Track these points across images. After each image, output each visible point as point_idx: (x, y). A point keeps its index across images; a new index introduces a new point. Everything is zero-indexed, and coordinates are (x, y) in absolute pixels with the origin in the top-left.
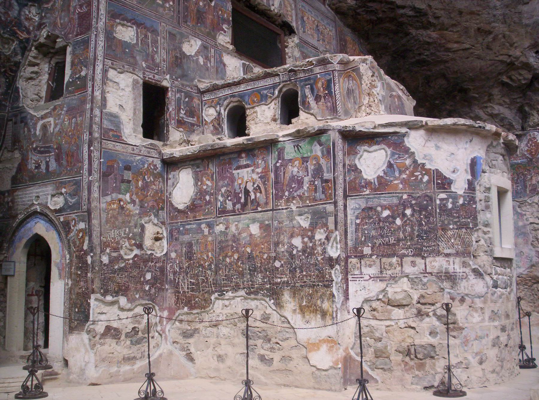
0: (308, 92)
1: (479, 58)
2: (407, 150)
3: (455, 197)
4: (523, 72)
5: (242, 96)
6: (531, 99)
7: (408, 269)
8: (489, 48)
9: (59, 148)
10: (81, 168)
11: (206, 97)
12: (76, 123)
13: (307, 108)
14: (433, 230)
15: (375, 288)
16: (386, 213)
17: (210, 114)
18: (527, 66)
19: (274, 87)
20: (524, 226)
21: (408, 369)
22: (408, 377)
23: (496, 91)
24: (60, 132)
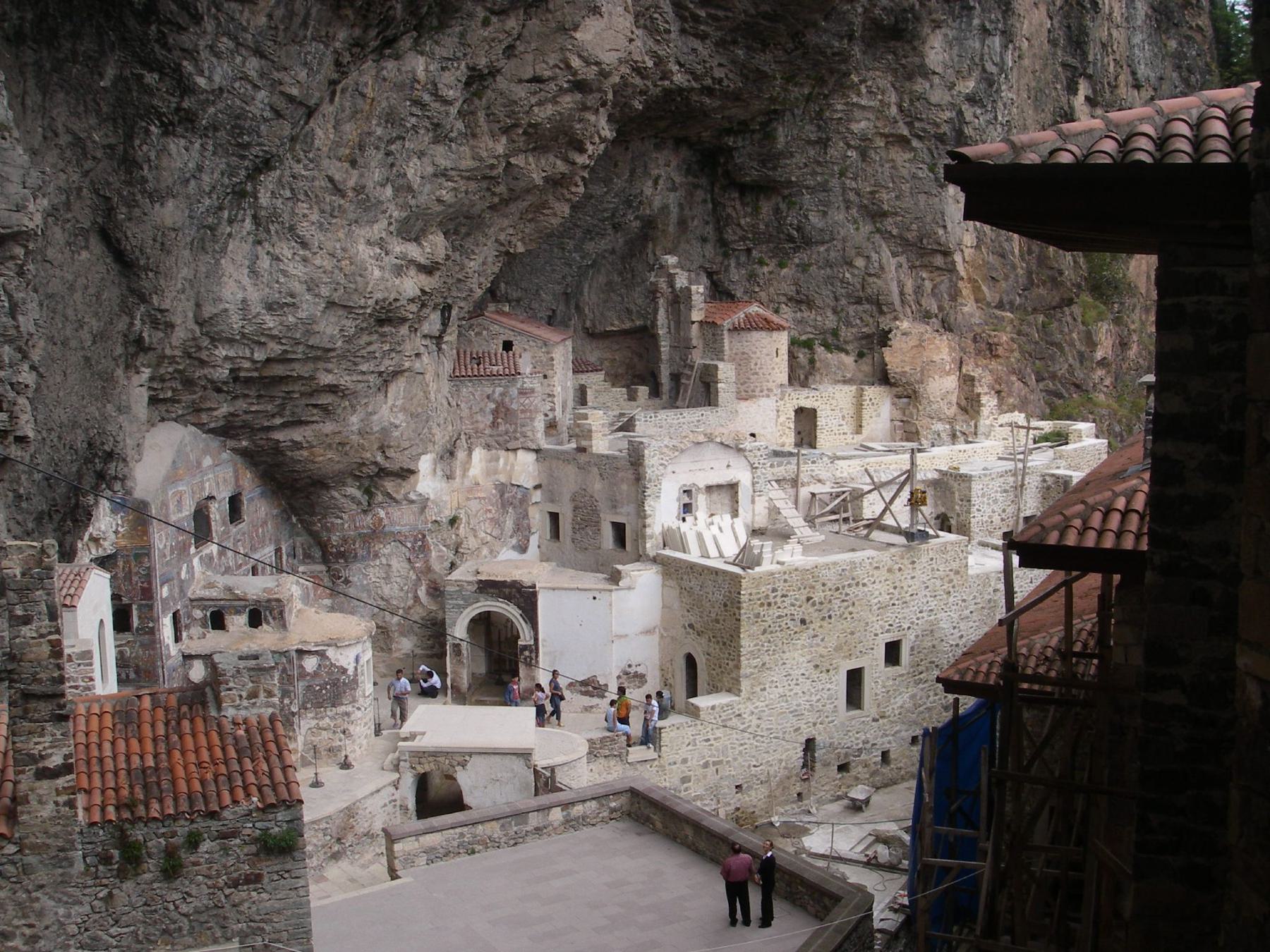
0: (268, 613)
1: (338, 462)
2: (327, 657)
3: (349, 677)
4: (372, 467)
5: (223, 607)
6: (376, 483)
7: (329, 713)
8: (346, 454)
9: (137, 666)
10: (158, 680)
11: (195, 603)
12: (150, 655)
13: (268, 623)
14: (340, 694)
15: (314, 723)
16: (318, 688)
17: (198, 614)
18: (376, 463)
19: (246, 607)
20: (368, 584)
21: (330, 757)
22: (330, 761)
23: (349, 481)
24: (135, 658)
